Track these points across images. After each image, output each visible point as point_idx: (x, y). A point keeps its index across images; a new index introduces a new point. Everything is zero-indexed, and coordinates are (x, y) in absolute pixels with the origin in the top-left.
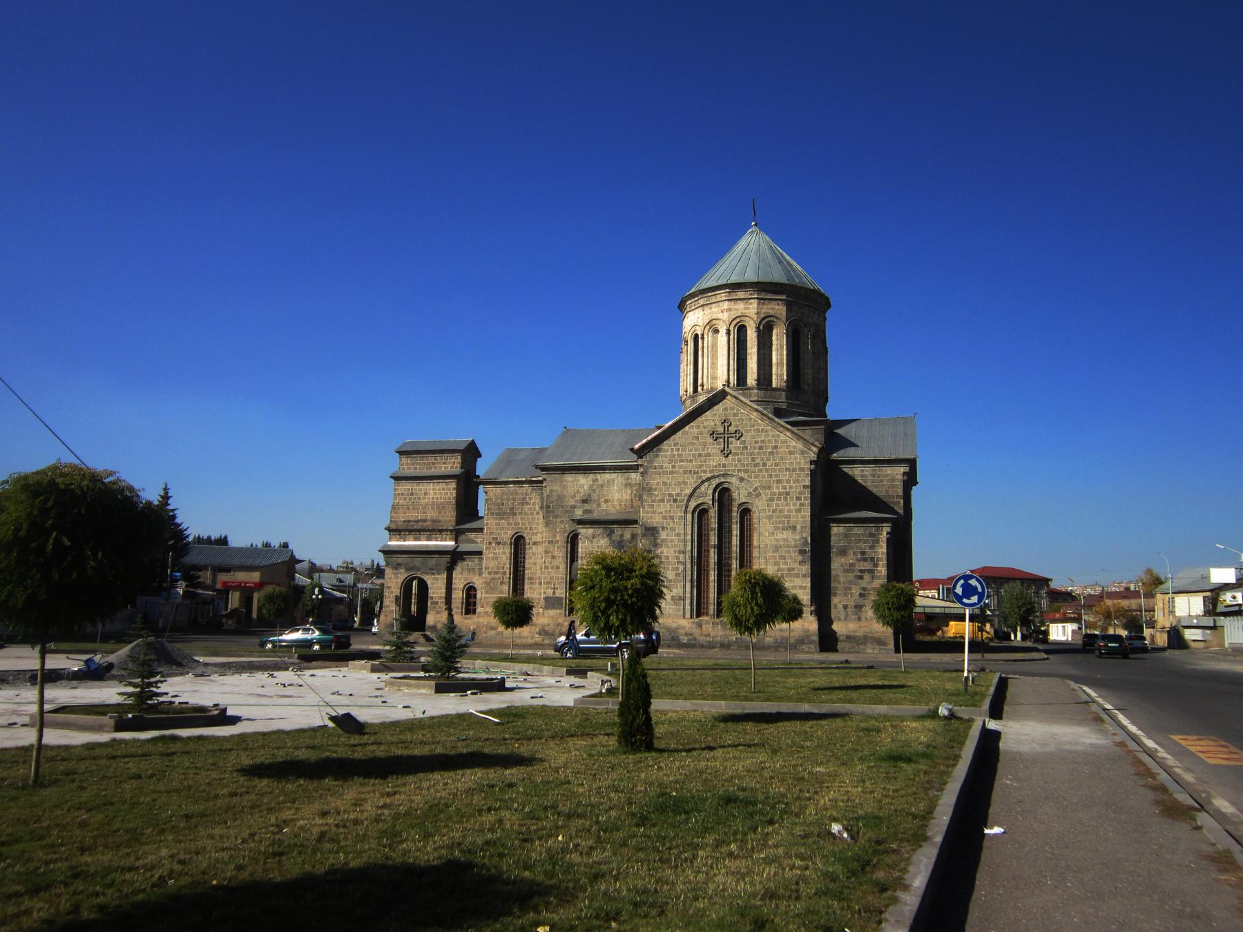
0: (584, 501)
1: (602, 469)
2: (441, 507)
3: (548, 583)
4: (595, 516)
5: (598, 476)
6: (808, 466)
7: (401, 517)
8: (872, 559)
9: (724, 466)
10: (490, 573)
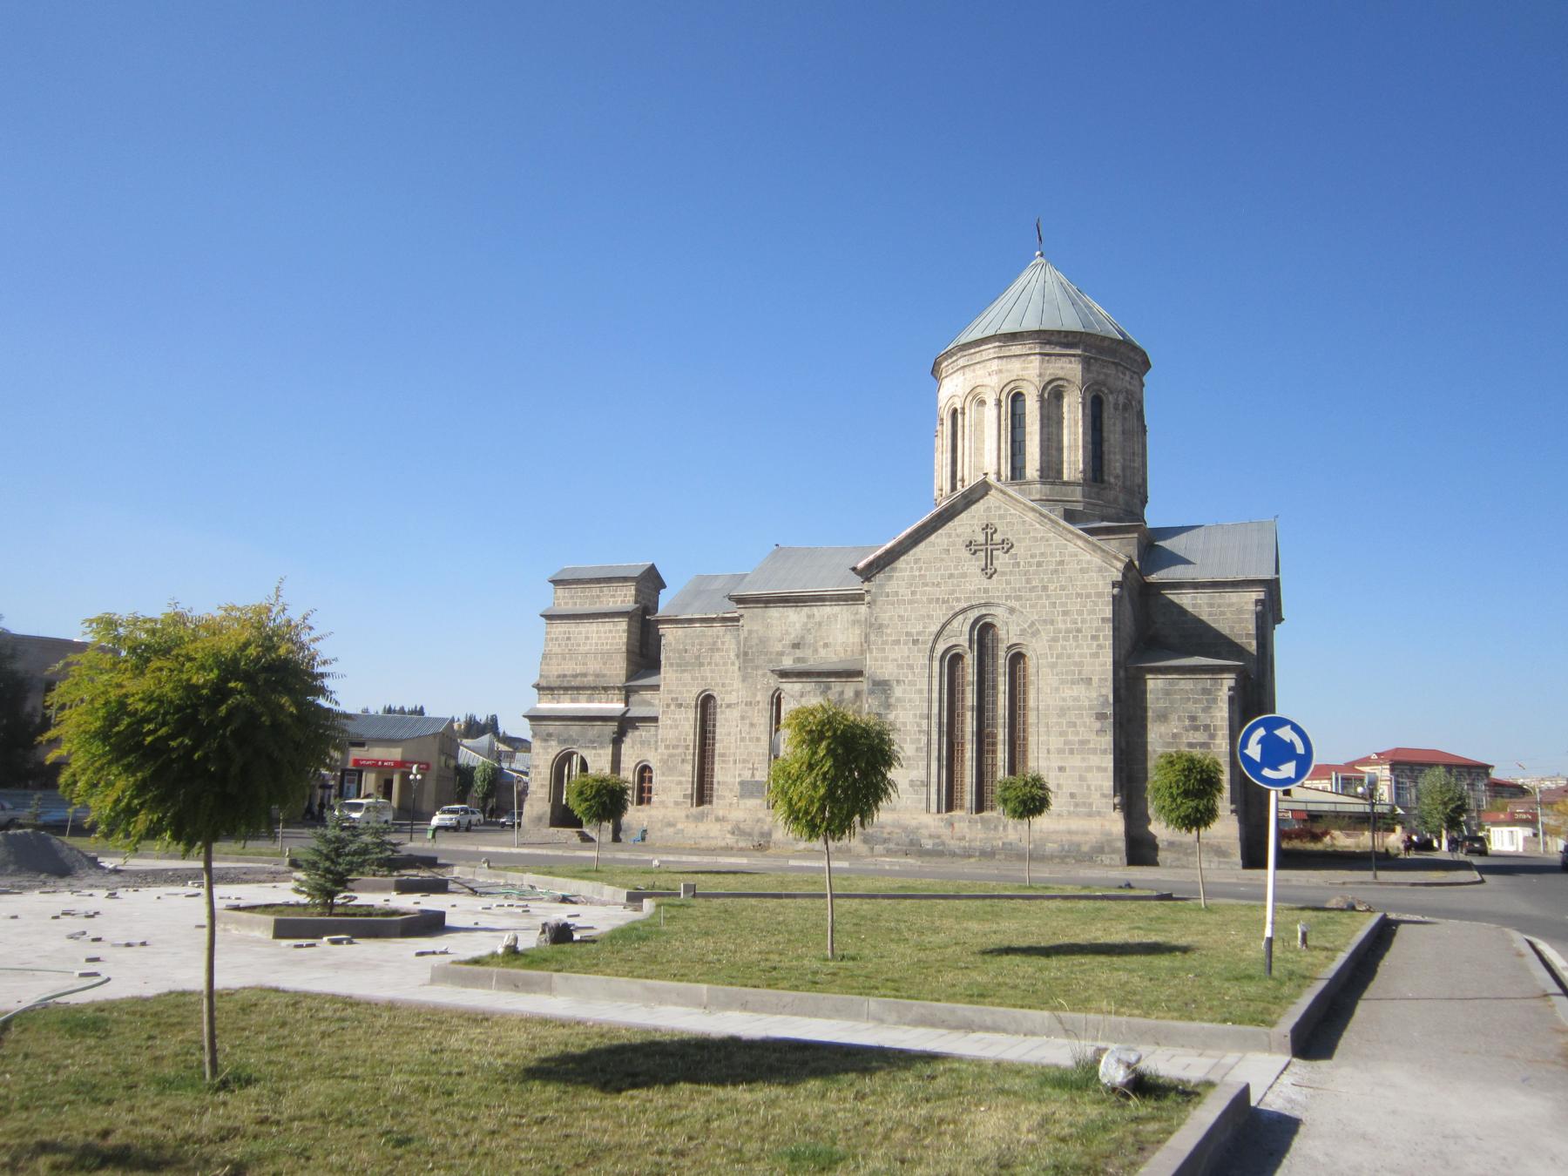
0: (796, 646)
1: (819, 599)
2: (606, 656)
3: (744, 761)
4: (811, 663)
6: (1109, 589)
7: (555, 670)
8: (1207, 727)
9: (986, 591)
10: (667, 747)
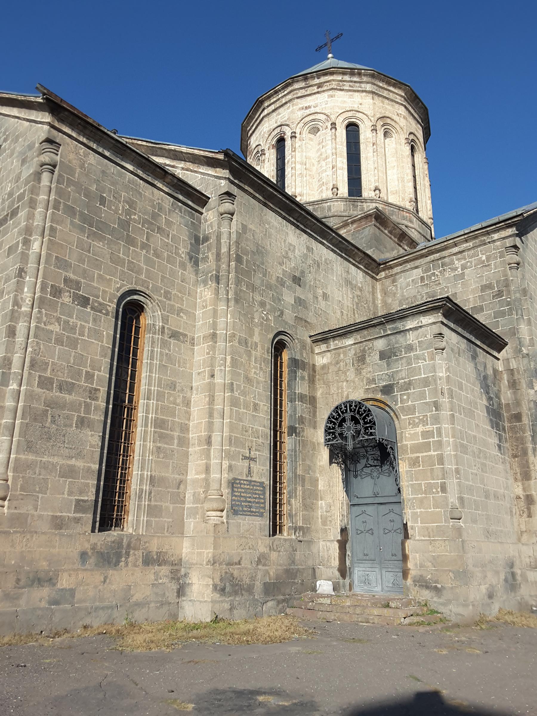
5: (314, 244)
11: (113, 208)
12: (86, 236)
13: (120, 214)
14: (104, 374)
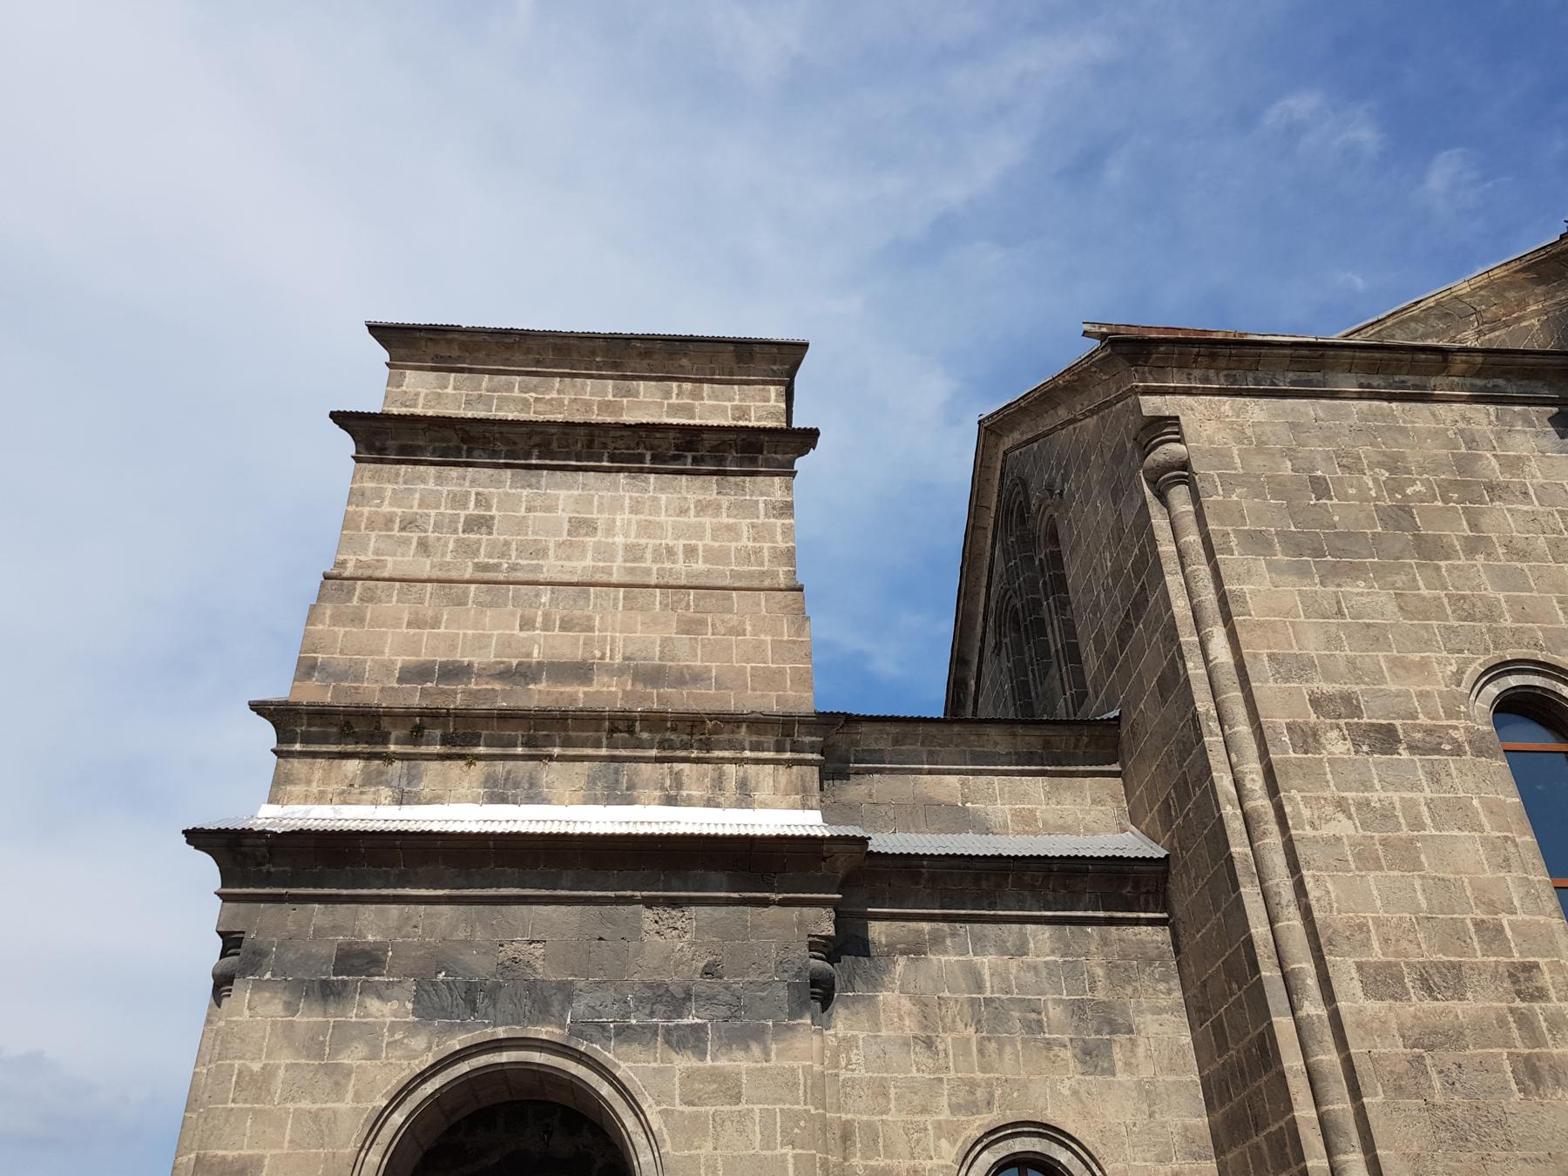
10: (1382, 981)
11: (1352, 491)
12: (1317, 580)
13: (1377, 499)
14: (1527, 918)
